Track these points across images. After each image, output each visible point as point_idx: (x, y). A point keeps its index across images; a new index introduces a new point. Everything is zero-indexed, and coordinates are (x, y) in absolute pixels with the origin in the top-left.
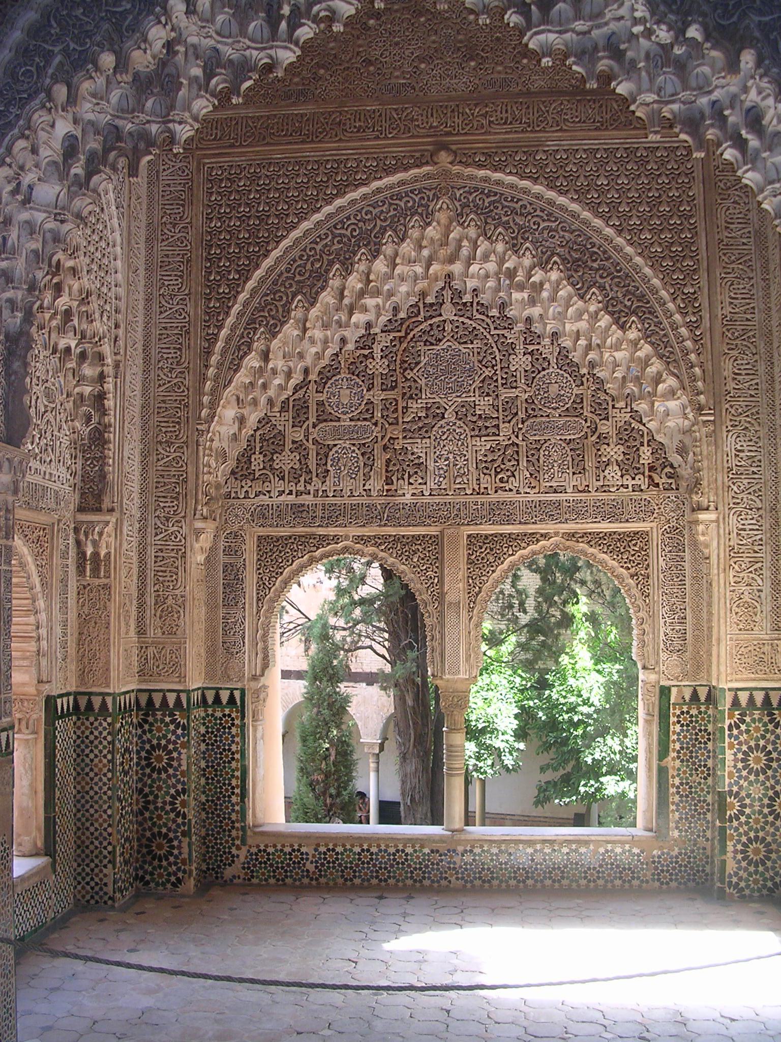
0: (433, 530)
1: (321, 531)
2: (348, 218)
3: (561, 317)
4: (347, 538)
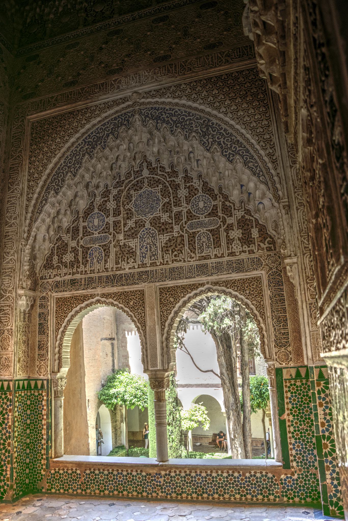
2: (92, 133)
4: (98, 295)
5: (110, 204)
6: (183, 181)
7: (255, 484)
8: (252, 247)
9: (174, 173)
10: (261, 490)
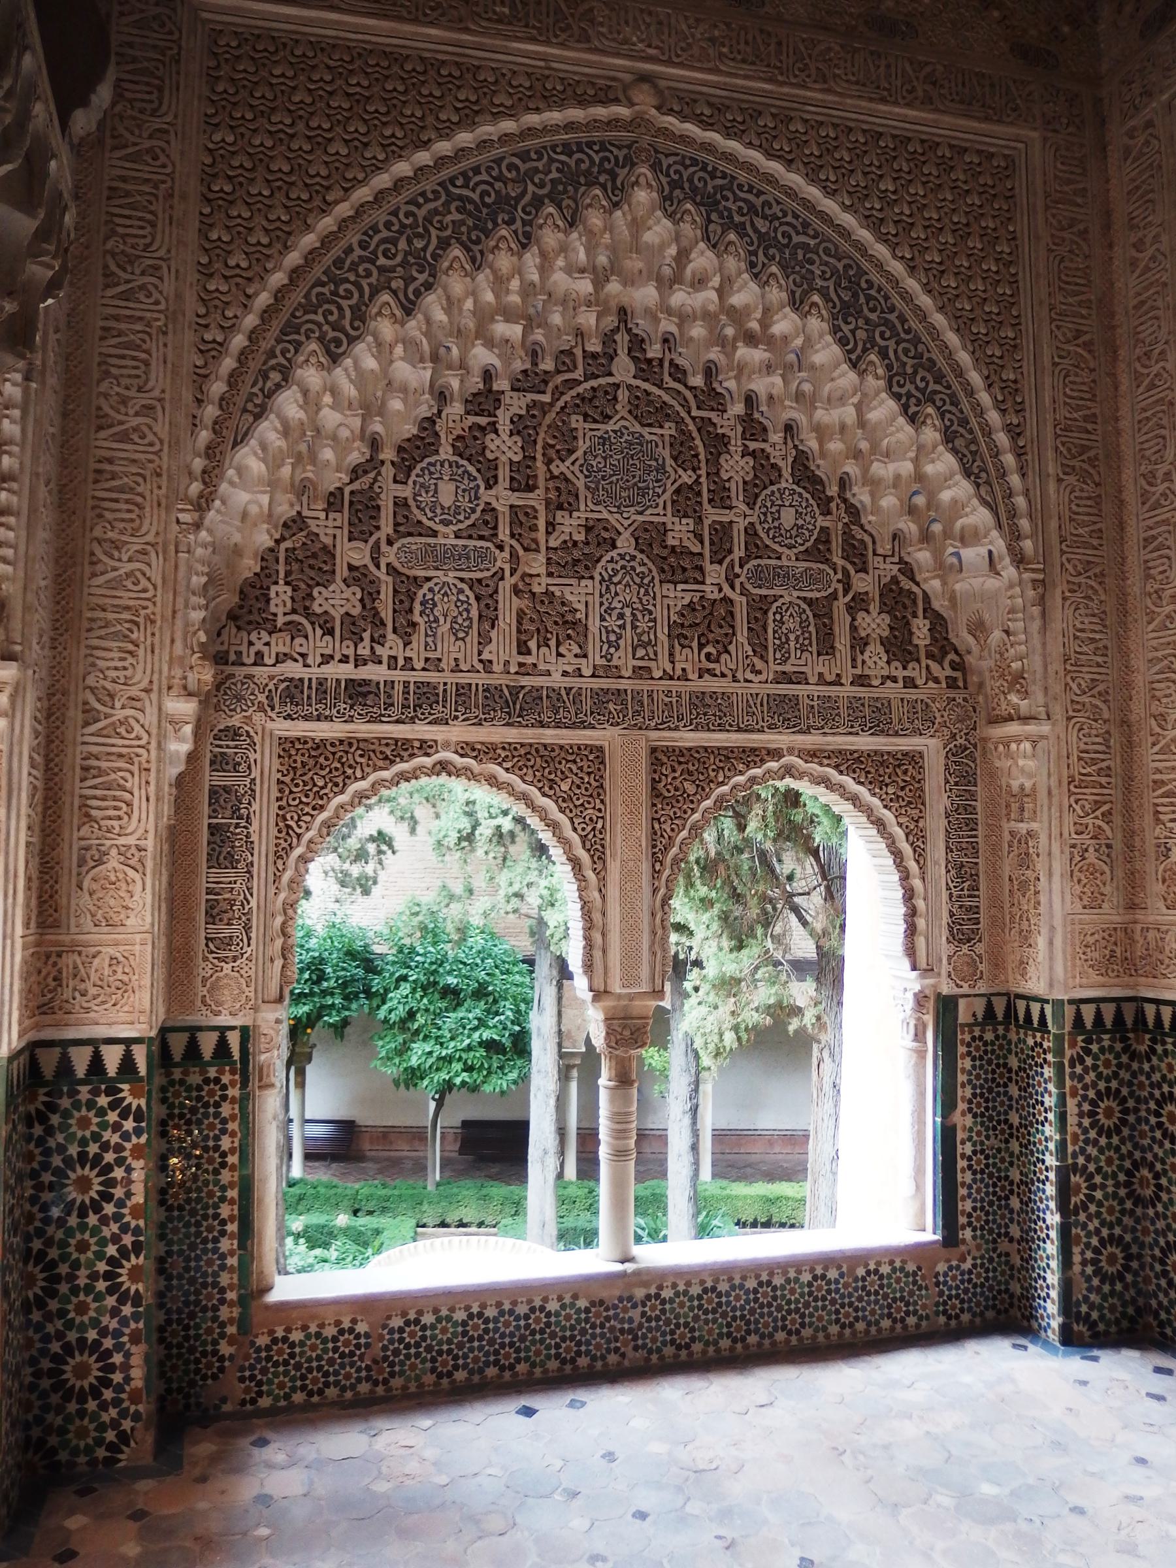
2: (477, 170)
4: (447, 745)
5: (498, 442)
6: (740, 429)
7: (876, 1293)
8: (913, 671)
9: (712, 397)
10: (889, 1306)
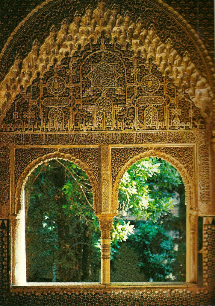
0: (96, 146)
1: (45, 147)
2: (59, 4)
3: (154, 50)
4: (57, 150)
6: (136, 61)
